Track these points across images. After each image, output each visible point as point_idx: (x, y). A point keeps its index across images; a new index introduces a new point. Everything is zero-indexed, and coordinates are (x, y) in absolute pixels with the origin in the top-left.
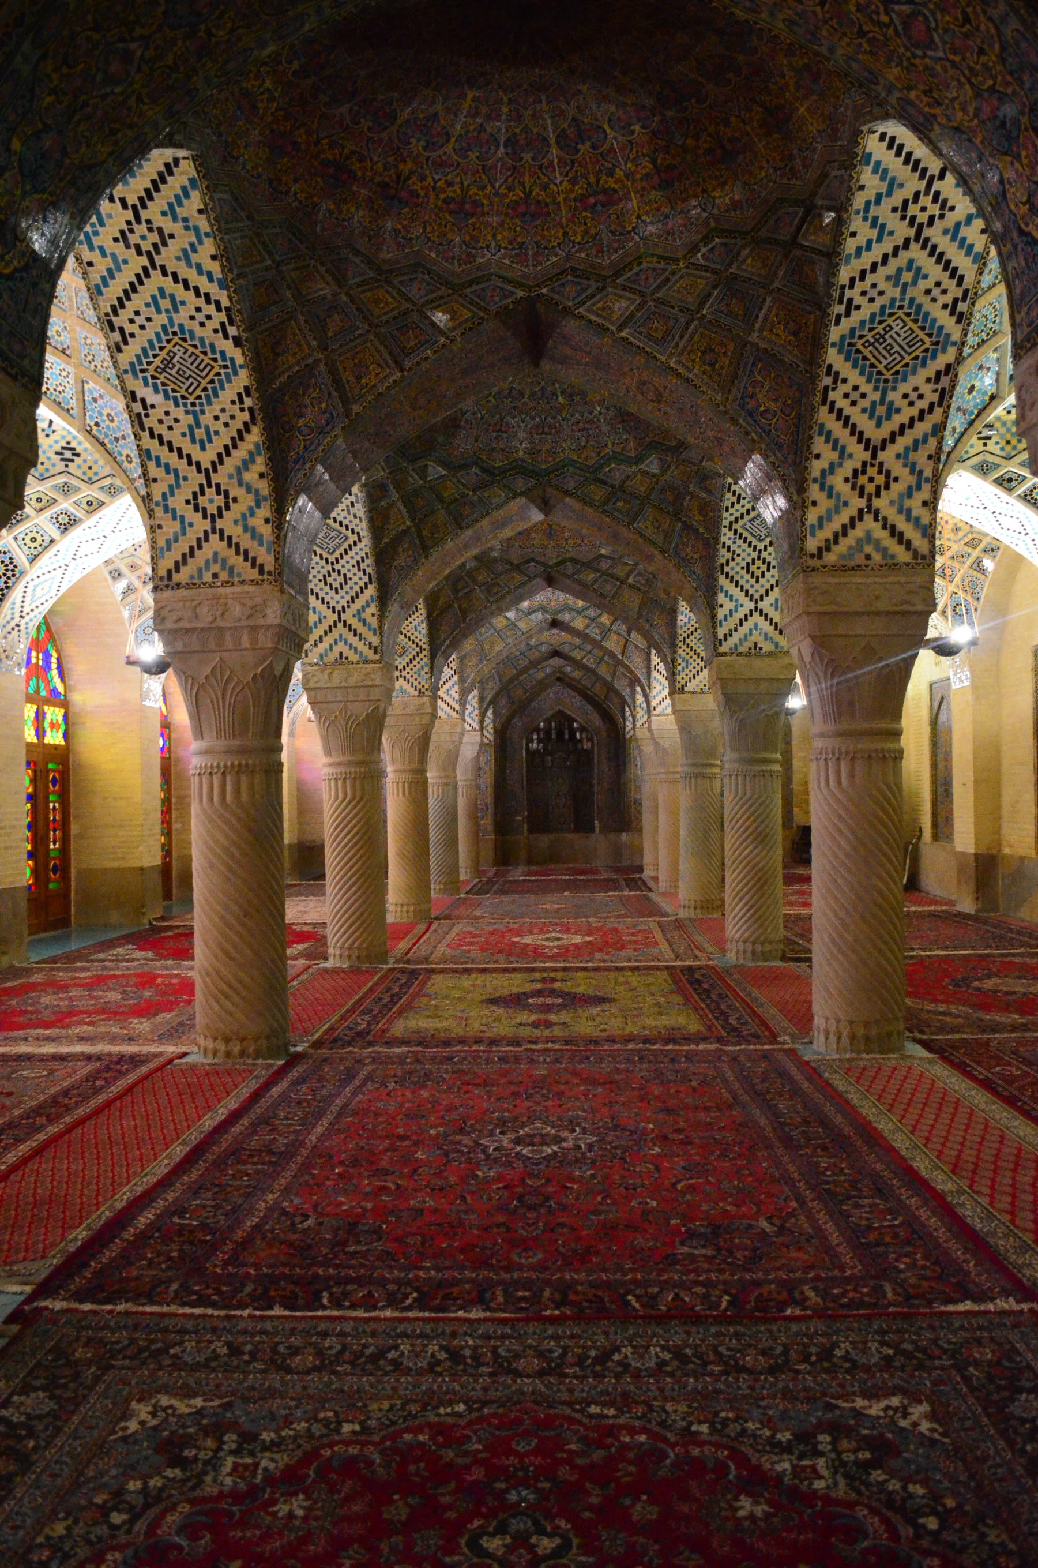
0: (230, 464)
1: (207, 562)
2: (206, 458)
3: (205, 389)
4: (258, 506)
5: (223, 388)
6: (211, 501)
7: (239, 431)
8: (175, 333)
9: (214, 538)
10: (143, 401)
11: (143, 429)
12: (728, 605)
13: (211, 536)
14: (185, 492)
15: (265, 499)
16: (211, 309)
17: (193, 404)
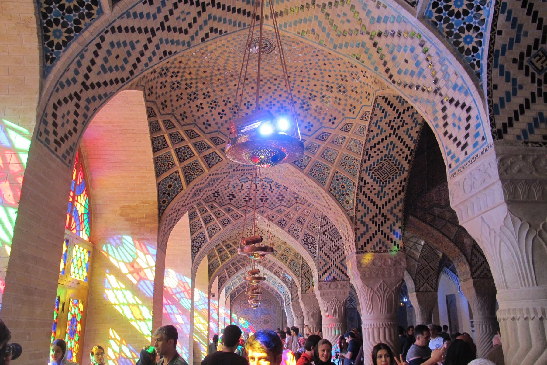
0: (389, 206)
1: (377, 243)
2: (380, 203)
3: (390, 178)
4: (397, 222)
5: (396, 178)
6: (379, 219)
7: (396, 194)
8: (388, 158)
9: (379, 234)
10: (365, 181)
11: (361, 192)
12: (475, 260)
13: (378, 233)
14: (370, 215)
15: (400, 219)
16: (405, 150)
17: (383, 183)
